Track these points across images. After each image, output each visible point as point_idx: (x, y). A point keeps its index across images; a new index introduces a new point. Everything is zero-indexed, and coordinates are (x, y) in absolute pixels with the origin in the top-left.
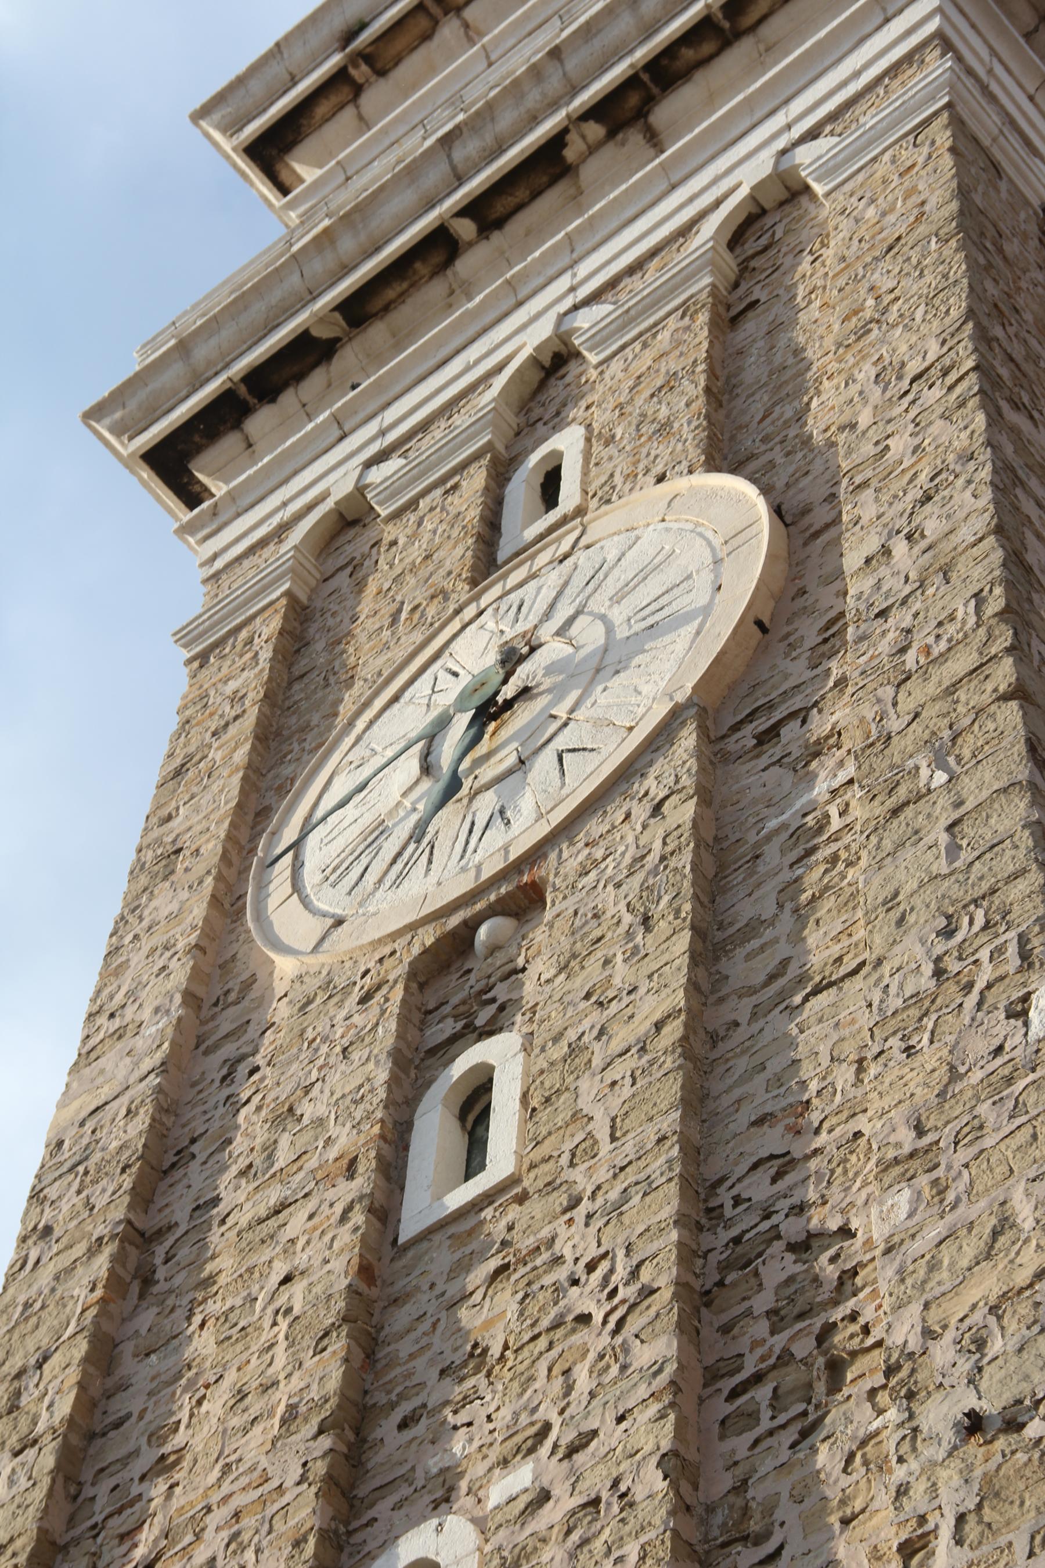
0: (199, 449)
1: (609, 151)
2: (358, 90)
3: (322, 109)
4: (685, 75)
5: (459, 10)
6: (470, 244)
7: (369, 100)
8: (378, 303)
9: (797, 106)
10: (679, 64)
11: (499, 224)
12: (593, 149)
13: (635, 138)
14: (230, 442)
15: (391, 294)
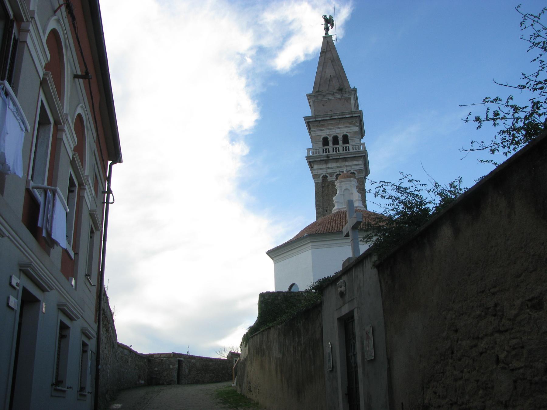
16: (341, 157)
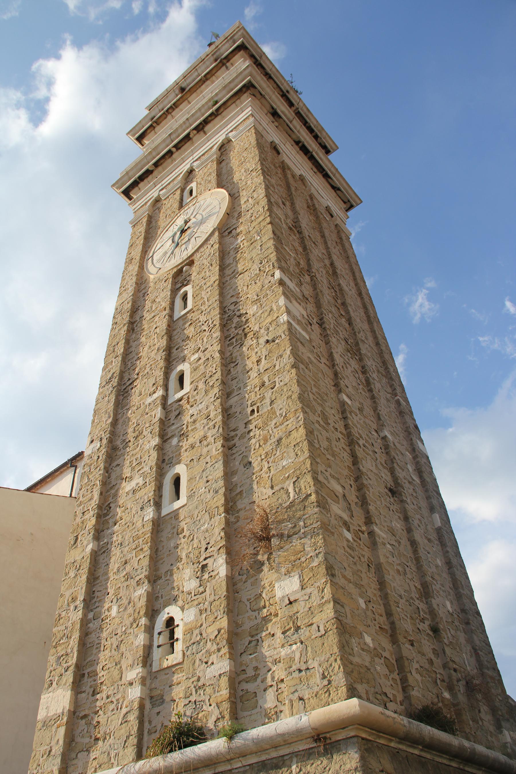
0: (131, 190)
1: (197, 135)
2: (154, 128)
3: (148, 131)
4: (210, 122)
5: (171, 113)
6: (175, 152)
7: (156, 129)
8: (160, 163)
9: (229, 127)
10: (208, 120)
11: (180, 148)
12: (195, 135)
13: (202, 133)
14: (136, 189)
15: (162, 161)
16: (314, 154)
